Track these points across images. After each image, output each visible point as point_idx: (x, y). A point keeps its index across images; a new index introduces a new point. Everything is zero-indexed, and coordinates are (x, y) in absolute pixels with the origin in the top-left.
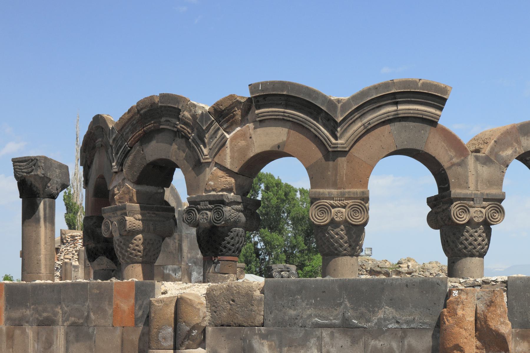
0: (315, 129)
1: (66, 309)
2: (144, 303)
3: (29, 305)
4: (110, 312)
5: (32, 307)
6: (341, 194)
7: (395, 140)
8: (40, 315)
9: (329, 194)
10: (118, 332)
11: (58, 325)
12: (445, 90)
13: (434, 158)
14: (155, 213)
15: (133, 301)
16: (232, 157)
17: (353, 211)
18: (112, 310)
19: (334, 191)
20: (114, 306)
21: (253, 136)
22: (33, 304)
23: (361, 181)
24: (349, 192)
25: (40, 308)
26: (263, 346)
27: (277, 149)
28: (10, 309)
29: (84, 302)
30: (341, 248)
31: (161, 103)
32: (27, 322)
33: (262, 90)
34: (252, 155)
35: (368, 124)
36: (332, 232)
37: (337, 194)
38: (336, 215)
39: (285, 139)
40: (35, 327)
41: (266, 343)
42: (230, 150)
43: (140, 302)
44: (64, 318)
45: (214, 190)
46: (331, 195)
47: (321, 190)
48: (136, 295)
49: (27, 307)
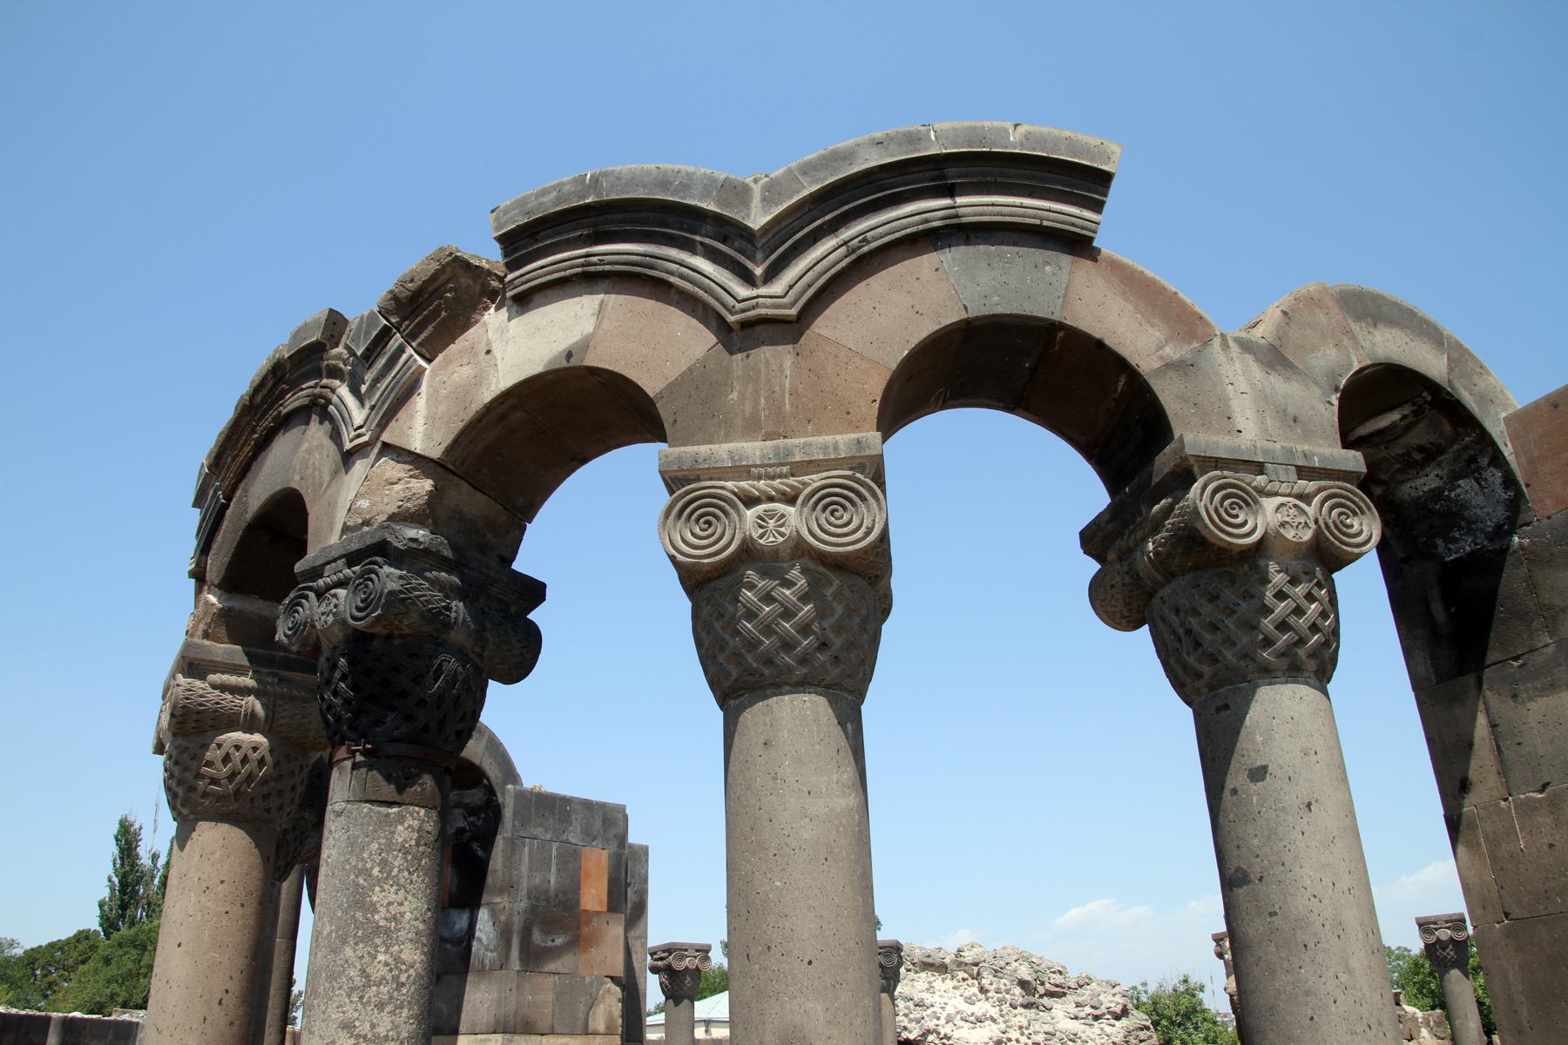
0: (682, 277)
6: (777, 454)
7: (960, 292)
9: (732, 458)
13: (1100, 344)
14: (275, 675)
17: (825, 508)
19: (753, 449)
23: (848, 413)
27: (564, 364)
30: (787, 653)
35: (860, 242)
36: (749, 594)
37: (763, 456)
38: (761, 527)
39: (589, 329)
42: (428, 399)
46: (740, 460)
47: (703, 449)
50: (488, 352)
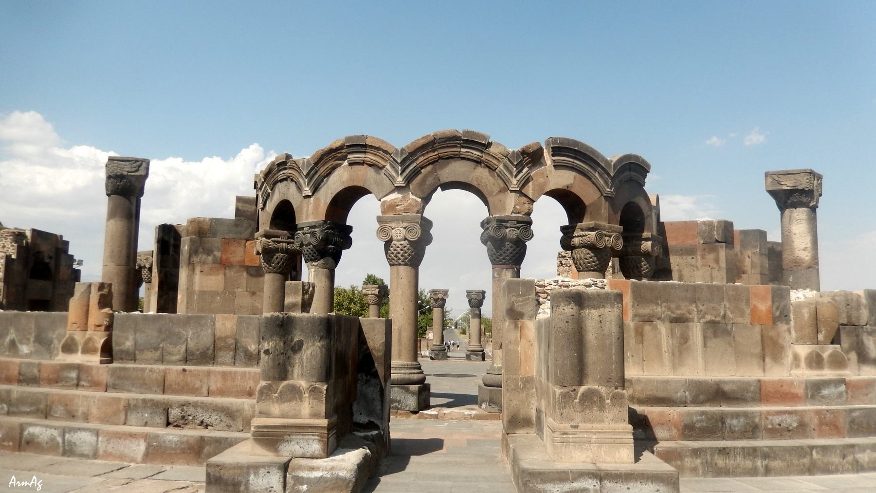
1: (701, 307)
2: (781, 304)
3: (660, 303)
4: (748, 311)
5: (664, 304)
8: (673, 312)
10: (757, 329)
11: (694, 321)
12: (649, 166)
15: (770, 303)
16: (532, 189)
18: (749, 310)
20: (752, 307)
21: (549, 176)
22: (664, 302)
24: (613, 226)
25: (673, 306)
26: (870, 341)
27: (566, 189)
28: (638, 305)
29: (720, 302)
31: (464, 136)
32: (659, 319)
33: (560, 143)
34: (548, 190)
39: (572, 182)
40: (668, 324)
41: (870, 338)
43: (777, 304)
44: (700, 316)
45: (519, 213)
48: (773, 297)
49: (657, 304)
50: (547, 177)
